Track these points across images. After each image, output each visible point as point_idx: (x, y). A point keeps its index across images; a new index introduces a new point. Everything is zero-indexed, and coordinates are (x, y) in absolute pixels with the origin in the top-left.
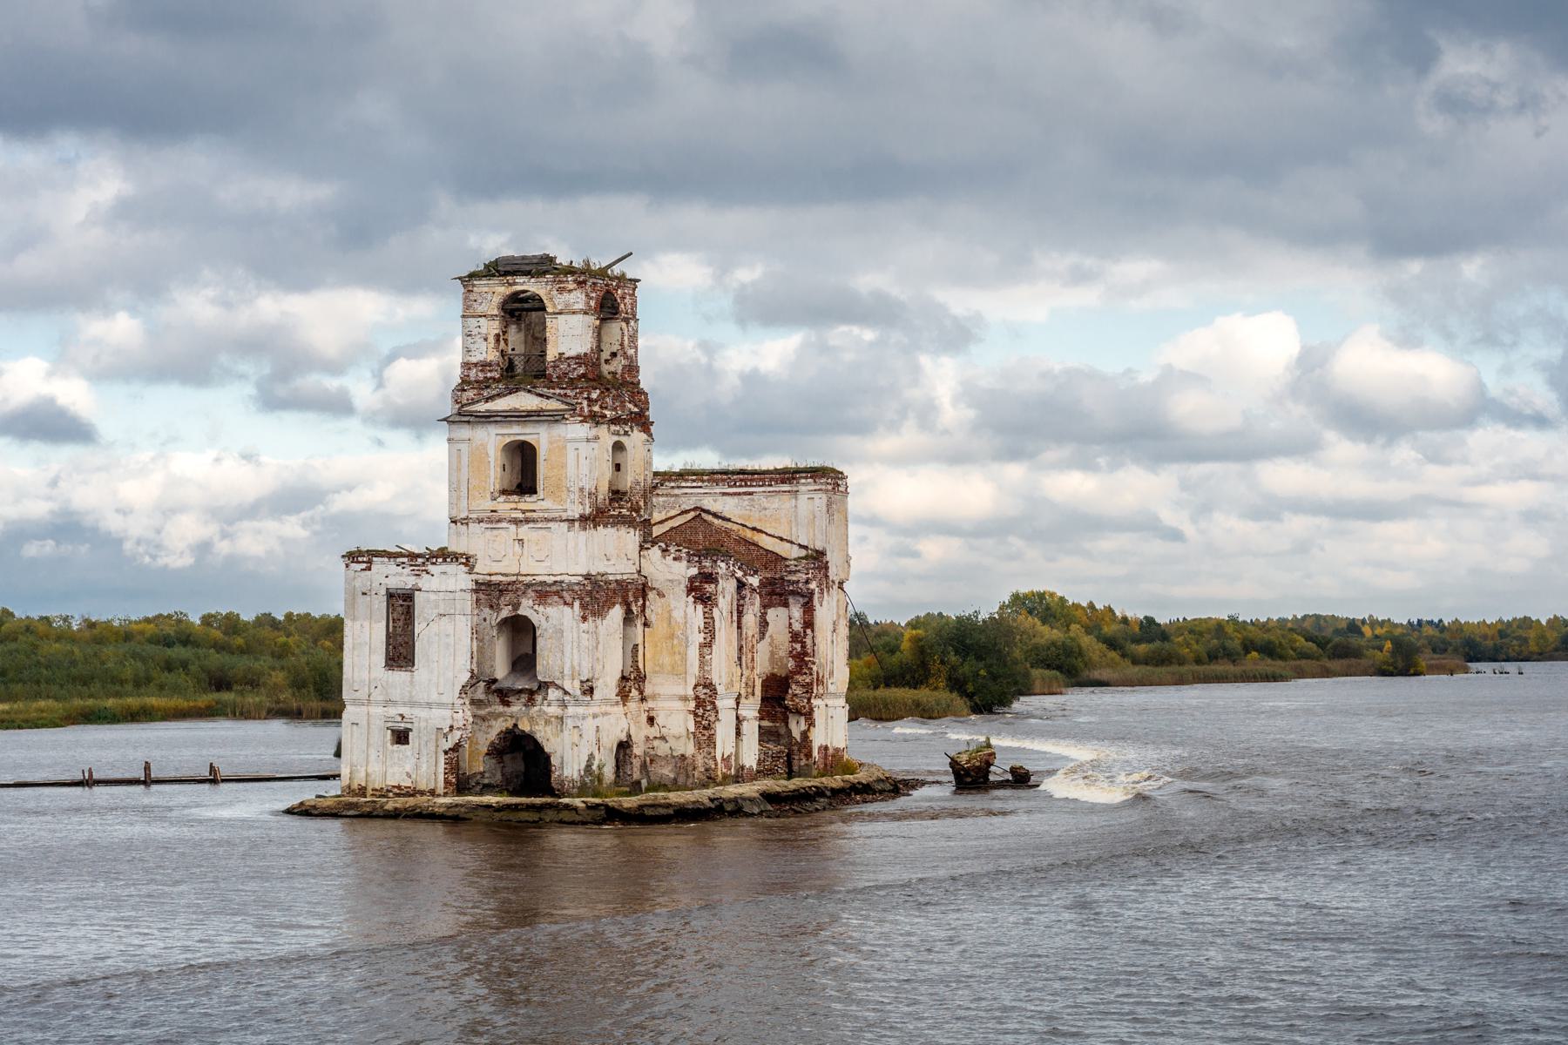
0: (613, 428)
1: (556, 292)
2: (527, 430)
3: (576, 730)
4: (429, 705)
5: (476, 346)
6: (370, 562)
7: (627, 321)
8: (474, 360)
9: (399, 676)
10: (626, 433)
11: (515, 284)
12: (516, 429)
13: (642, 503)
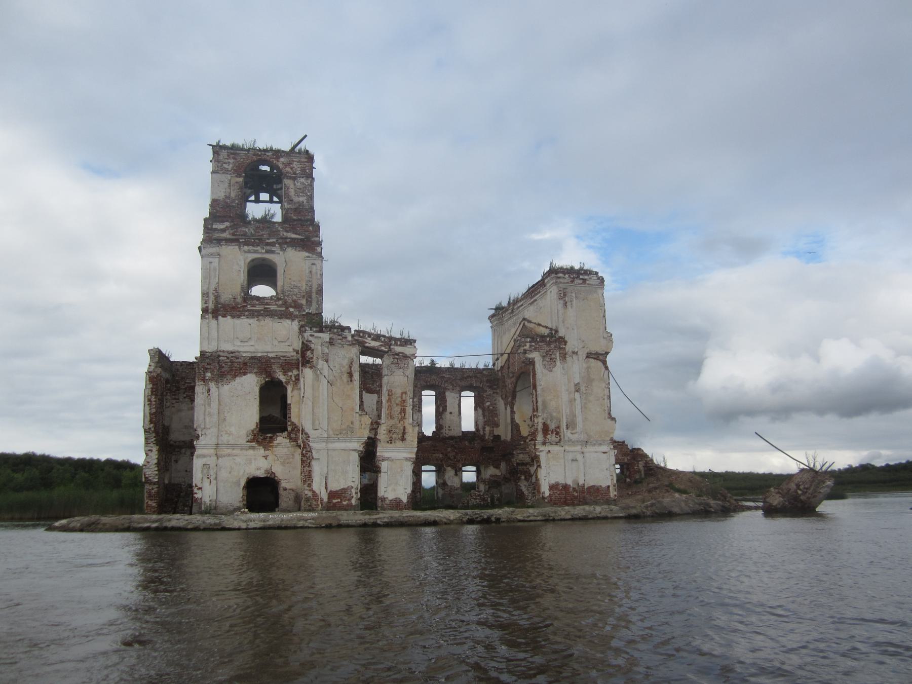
0: (246, 248)
7: (294, 179)
10: (267, 252)
13: (304, 302)
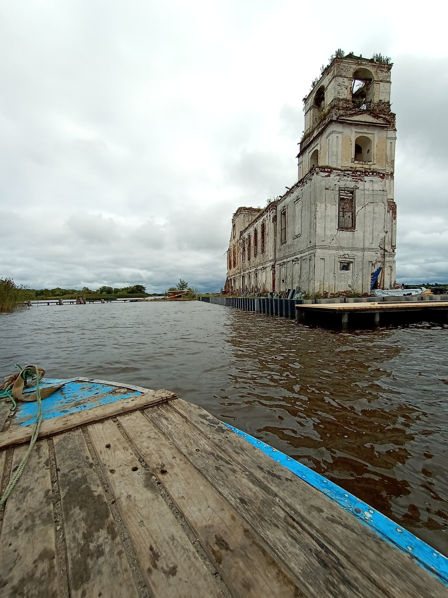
1: (379, 71)
2: (369, 132)
3: (390, 267)
4: (363, 249)
5: (342, 91)
6: (330, 172)
8: (341, 97)
9: (347, 234)
11: (361, 64)
12: (365, 130)
